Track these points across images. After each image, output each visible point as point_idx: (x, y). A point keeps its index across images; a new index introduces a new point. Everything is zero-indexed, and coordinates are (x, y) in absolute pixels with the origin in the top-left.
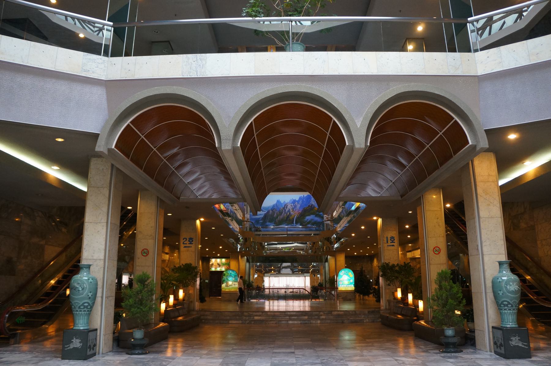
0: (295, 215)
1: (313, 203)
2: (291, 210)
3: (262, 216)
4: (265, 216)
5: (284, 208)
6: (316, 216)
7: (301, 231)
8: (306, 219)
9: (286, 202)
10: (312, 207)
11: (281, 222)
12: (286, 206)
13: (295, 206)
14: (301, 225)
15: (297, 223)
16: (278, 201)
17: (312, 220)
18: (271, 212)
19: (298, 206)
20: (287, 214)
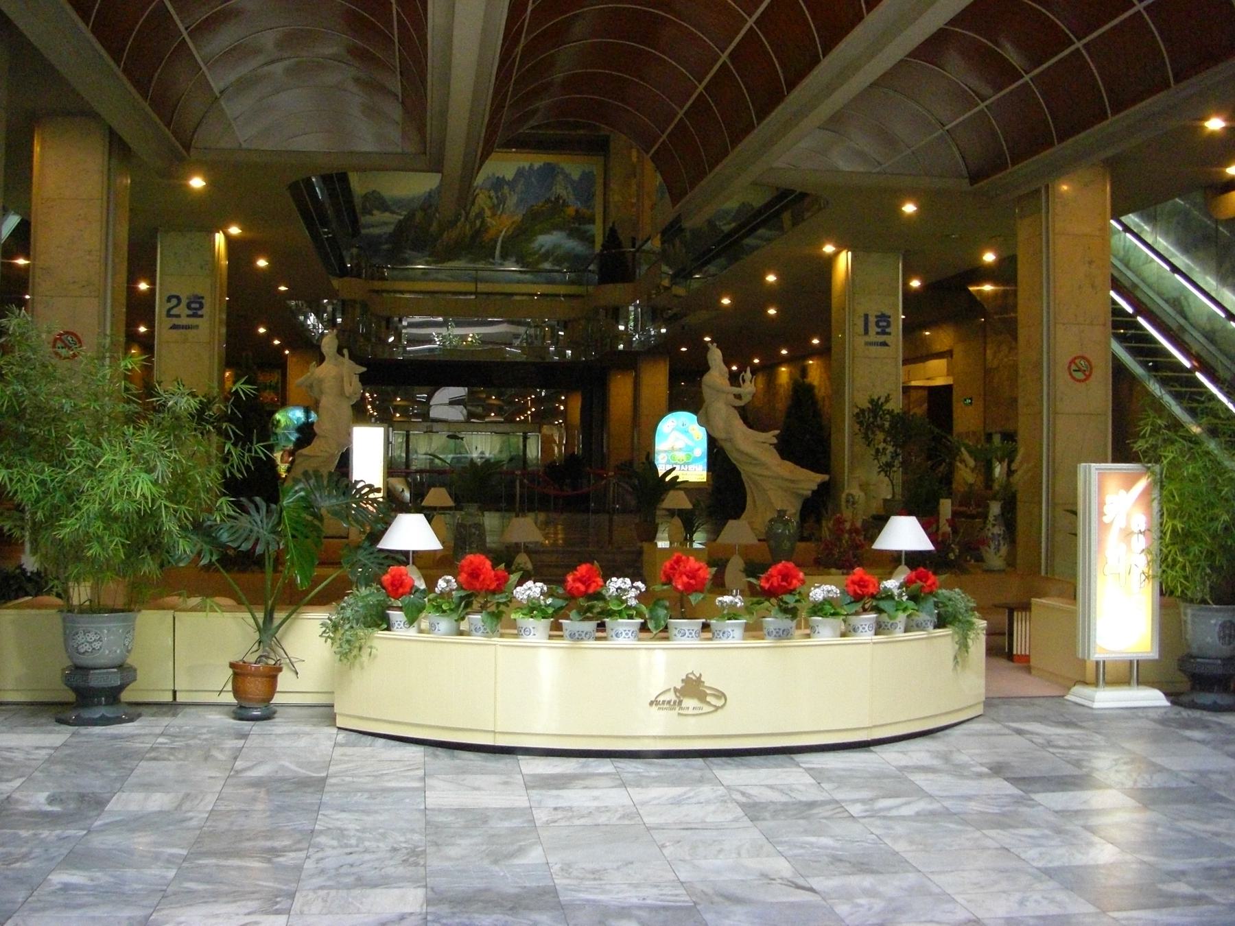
0: (502, 225)
1: (563, 193)
2: (488, 213)
3: (390, 229)
4: (401, 228)
7: (519, 282)
8: (536, 245)
10: (557, 205)
11: (451, 253)
13: (502, 200)
14: (517, 262)
15: (504, 256)
17: (556, 246)
18: (419, 216)
19: (512, 200)
20: (473, 224)
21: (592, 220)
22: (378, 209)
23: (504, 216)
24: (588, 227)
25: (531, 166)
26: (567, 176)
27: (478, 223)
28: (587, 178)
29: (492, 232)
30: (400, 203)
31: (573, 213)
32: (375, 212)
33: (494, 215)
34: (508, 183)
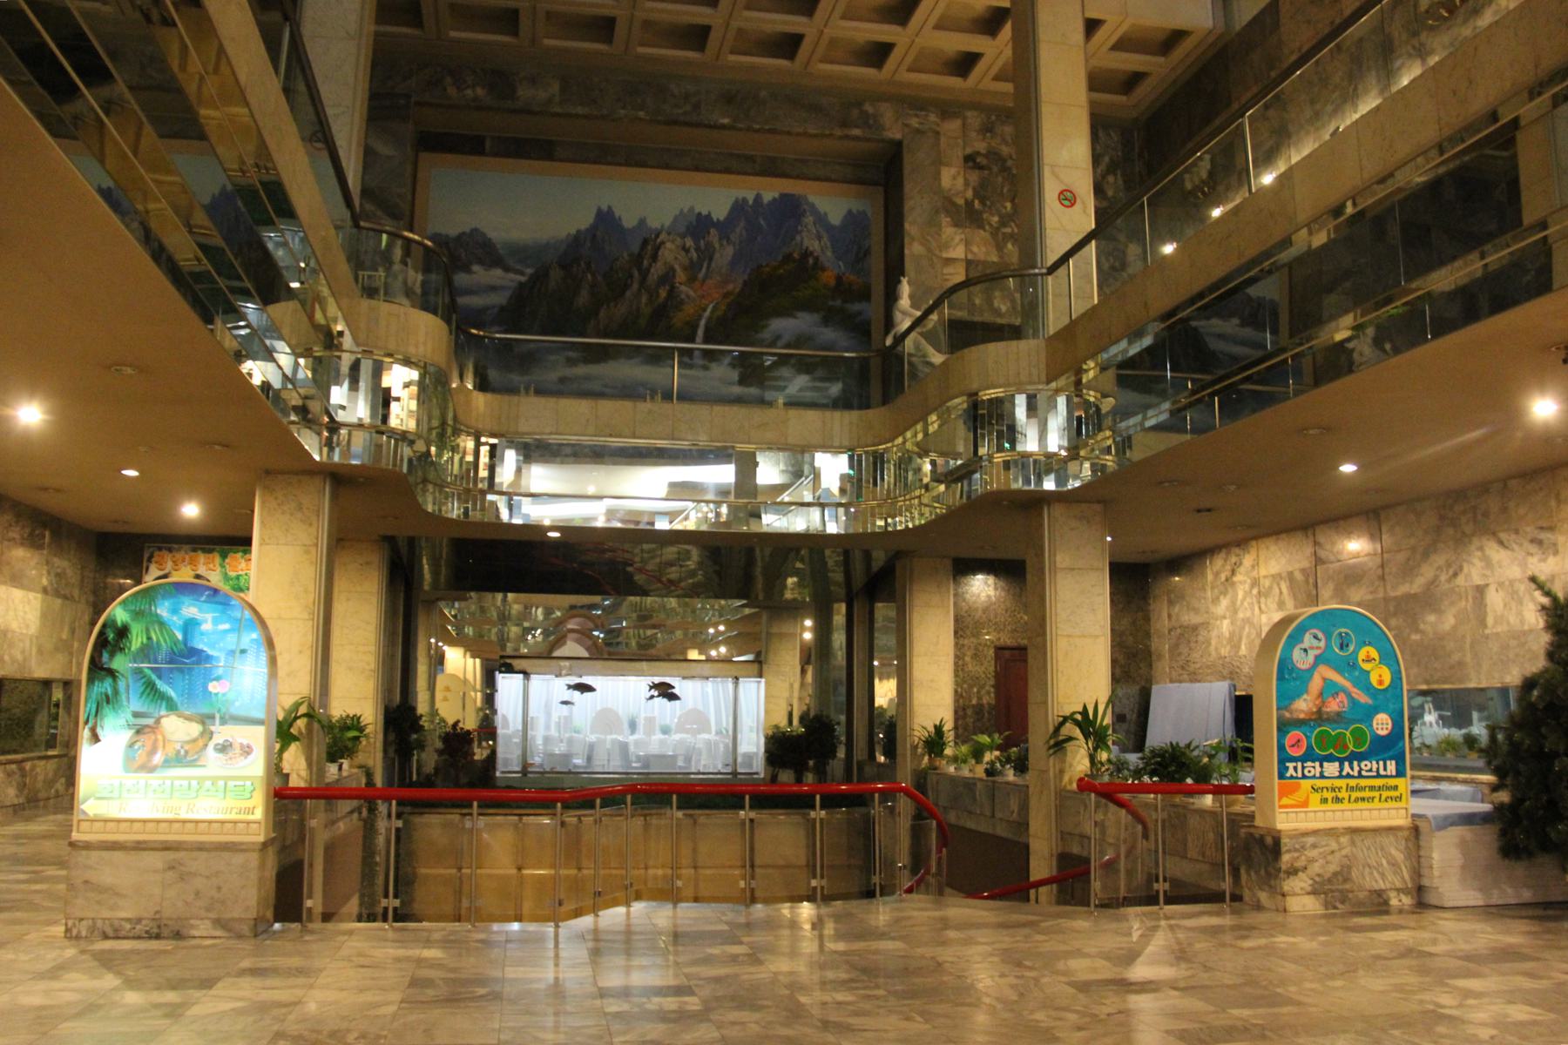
1: (814, 245)
2: (681, 276)
3: (498, 299)
5: (637, 259)
6: (826, 321)
9: (654, 223)
10: (805, 267)
12: (650, 244)
13: (707, 254)
16: (605, 218)
18: (556, 275)
19: (725, 254)
21: (865, 295)
22: (481, 262)
23: (709, 282)
24: (856, 307)
25: (758, 197)
26: (821, 219)
27: (663, 293)
28: (855, 221)
29: (689, 309)
30: (522, 253)
31: (833, 283)
32: (476, 268)
33: (692, 279)
34: (717, 225)
